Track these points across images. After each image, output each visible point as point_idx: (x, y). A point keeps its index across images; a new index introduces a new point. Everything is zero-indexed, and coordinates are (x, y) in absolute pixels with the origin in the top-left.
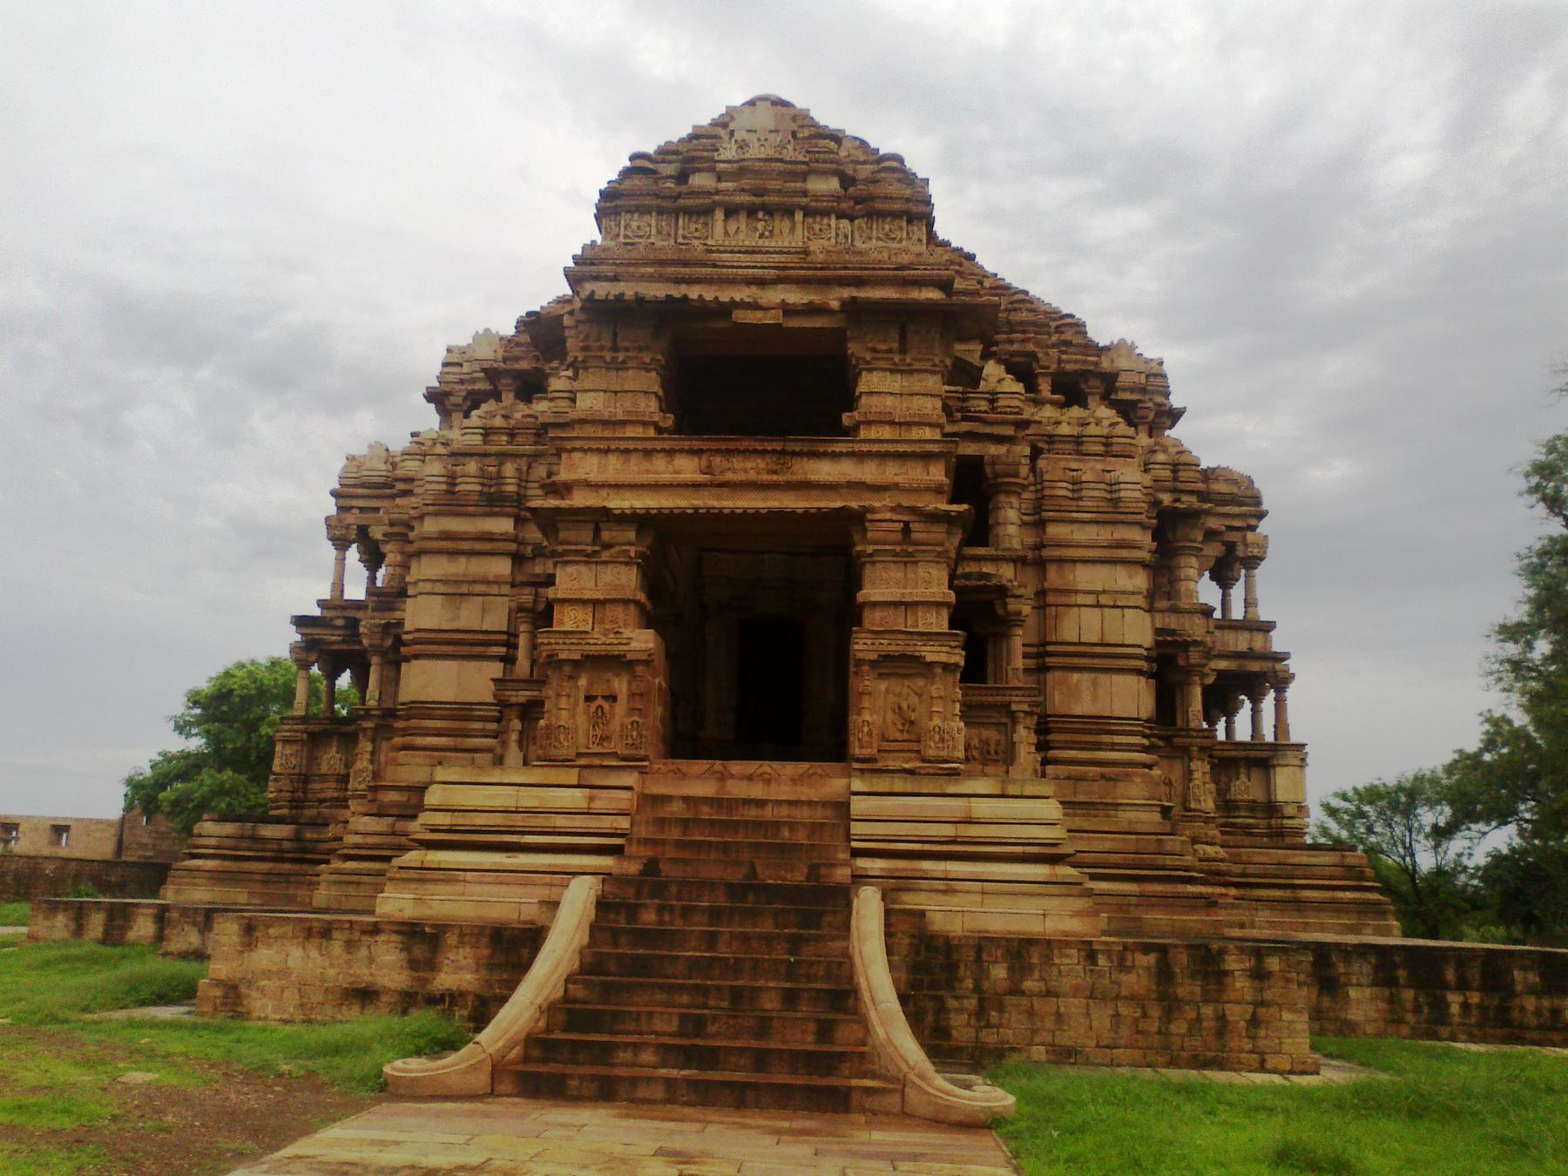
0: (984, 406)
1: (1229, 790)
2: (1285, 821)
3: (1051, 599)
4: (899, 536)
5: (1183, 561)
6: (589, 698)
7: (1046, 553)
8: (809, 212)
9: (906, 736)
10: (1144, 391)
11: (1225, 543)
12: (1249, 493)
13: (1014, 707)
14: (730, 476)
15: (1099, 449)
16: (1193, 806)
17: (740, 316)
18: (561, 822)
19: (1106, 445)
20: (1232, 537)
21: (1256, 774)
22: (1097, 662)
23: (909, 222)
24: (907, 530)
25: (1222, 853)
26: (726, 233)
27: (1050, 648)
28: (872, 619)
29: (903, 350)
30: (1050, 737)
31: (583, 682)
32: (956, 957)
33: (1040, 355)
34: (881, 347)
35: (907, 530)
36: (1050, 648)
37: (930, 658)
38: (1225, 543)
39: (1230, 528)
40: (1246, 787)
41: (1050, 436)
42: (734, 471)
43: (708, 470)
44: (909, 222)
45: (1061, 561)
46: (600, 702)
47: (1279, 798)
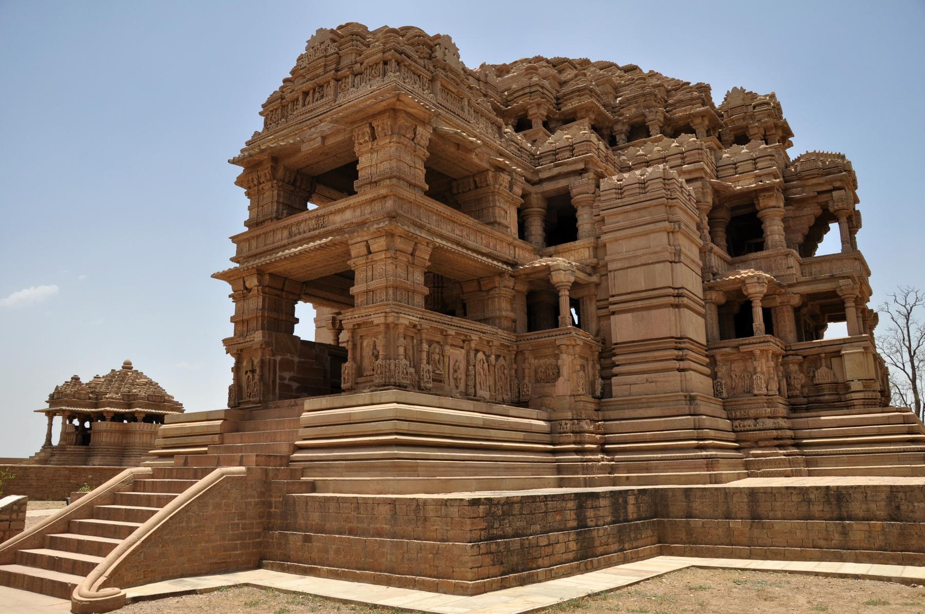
0: (568, 154)
1: (814, 377)
2: (853, 395)
3: (611, 266)
4: (364, 250)
5: (767, 223)
6: (246, 372)
7: (604, 238)
8: (337, 80)
9: (372, 373)
10: (752, 117)
11: (819, 204)
12: (832, 165)
13: (558, 343)
14: (298, 238)
15: (679, 162)
16: (756, 392)
17: (306, 148)
18: (198, 440)
19: (683, 158)
20: (823, 198)
21: (835, 361)
22: (639, 304)
23: (385, 63)
24: (368, 247)
25: (782, 423)
26: (304, 105)
27: (611, 299)
28: (358, 301)
29: (374, 137)
30: (614, 359)
31: (245, 364)
32: (297, 508)
33: (647, 114)
34: (361, 141)
35: (368, 247)
36: (611, 299)
37: (375, 322)
38: (819, 204)
39: (819, 193)
40: (823, 375)
41: (648, 162)
42: (300, 233)
43: (291, 235)
44: (385, 63)
45: (616, 240)
46: (249, 374)
47: (849, 377)
